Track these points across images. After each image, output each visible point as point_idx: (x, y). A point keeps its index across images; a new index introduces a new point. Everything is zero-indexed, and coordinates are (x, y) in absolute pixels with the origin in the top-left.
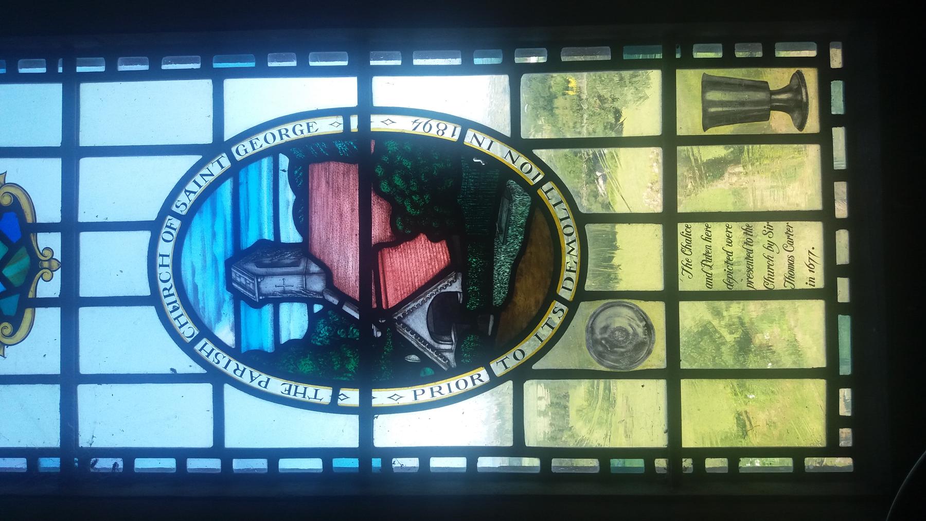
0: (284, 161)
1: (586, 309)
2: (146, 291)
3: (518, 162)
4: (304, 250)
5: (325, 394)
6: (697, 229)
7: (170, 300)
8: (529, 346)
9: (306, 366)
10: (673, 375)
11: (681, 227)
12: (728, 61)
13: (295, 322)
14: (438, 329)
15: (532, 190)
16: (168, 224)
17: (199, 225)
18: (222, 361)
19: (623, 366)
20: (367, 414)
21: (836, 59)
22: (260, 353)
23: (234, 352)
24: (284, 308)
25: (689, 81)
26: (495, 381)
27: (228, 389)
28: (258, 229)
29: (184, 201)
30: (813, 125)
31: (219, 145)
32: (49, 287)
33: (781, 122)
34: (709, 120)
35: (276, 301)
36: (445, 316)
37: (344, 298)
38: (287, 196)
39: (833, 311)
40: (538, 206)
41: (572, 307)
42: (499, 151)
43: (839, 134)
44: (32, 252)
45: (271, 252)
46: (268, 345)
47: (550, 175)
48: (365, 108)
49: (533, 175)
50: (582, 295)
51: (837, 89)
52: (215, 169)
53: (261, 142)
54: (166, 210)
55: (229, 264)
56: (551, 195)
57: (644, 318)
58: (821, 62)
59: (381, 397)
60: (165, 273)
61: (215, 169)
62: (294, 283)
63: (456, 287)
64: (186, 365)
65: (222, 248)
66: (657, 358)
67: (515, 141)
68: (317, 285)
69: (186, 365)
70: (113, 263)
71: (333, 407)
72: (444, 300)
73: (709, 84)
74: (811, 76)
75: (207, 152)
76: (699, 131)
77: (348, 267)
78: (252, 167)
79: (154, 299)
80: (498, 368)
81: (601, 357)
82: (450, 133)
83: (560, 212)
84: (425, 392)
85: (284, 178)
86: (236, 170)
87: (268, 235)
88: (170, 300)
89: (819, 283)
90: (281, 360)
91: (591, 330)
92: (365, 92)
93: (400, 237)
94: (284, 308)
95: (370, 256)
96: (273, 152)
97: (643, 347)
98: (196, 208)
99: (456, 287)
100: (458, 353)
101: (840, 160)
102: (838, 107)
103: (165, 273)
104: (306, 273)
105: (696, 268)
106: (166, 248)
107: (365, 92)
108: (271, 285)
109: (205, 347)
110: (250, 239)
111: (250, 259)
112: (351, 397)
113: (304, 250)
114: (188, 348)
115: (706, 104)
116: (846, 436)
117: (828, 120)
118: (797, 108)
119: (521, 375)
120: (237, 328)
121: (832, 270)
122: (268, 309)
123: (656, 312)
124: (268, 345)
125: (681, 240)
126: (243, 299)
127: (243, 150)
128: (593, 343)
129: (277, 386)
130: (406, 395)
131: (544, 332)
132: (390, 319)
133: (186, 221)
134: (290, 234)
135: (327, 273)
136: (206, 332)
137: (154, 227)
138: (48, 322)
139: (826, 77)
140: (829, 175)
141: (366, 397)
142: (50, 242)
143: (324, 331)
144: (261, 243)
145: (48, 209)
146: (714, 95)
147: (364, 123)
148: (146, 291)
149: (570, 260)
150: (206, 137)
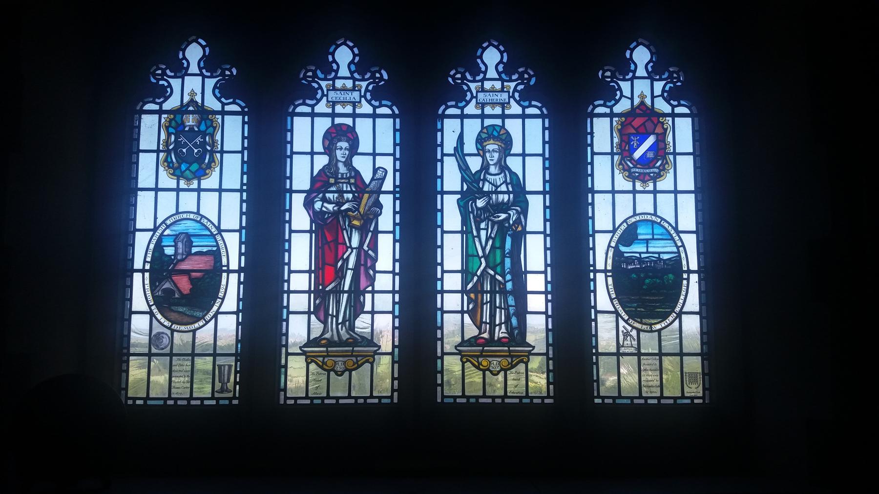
0: (215, 249)
1: (169, 332)
2: (180, 210)
3: (211, 314)
4: (189, 254)
5: (149, 259)
6: (189, 363)
7: (177, 217)
8: (159, 316)
9: (156, 254)
10: (150, 355)
11: (190, 358)
12: (236, 372)
13: (169, 251)
14: (165, 291)
15: (203, 318)
16: (199, 216)
17: (198, 225)
18: (159, 231)
19: (153, 341)
20: (143, 271)
21: (235, 402)
22: (161, 242)
23: (162, 235)
24: (173, 248)
25: (231, 361)
26: (150, 306)
27: (151, 233)
28: (196, 241)
29: (205, 221)
30: (217, 395)
31: (220, 231)
32: (183, 184)
33: (218, 386)
34: (220, 367)
35: (176, 246)
36: (169, 292)
37: (175, 265)
38: (205, 249)
39: (165, 399)
40: (198, 319)
41: (169, 328)
42: (215, 308)
43: (214, 402)
44: (193, 179)
45: (189, 244)
46: (163, 244)
47: (207, 322)
48: (229, 272)
49: (208, 318)
50: (173, 331)
51: (227, 402)
52: (214, 230)
53: (221, 243)
54: (203, 216)
55: (187, 233)
56: (201, 323)
57: (166, 347)
58: (234, 397)
59: (147, 275)
60: (185, 216)
61: (214, 230)
62: (180, 251)
63: (177, 296)
64: (159, 222)
65: (191, 231)
66: (154, 350)
67: (218, 313)
68: (179, 257)
69: (159, 222)
70: (188, 201)
71: (145, 262)
72: (173, 292)
73: (230, 366)
74: (231, 395)
75: (218, 228)
76: (217, 363)
77: (184, 266)
78: (213, 240)
79: (178, 213)
80: (153, 307)
81: (155, 336)
82: (221, 295)
83: (196, 325)
84: (147, 287)
85: (210, 248)
86: (213, 235)
87: (194, 244)
88: (177, 217)
89: (173, 396)
90: (159, 247)
91: (163, 333)
92: (234, 271)
93: (192, 280)
94: (173, 248)
95: (187, 272)
96: (217, 246)
97: (157, 347)
98: (203, 225)
99: (177, 296)
100: (158, 296)
101: (206, 402)
102: (221, 402)
103: (185, 216)
104: (183, 254)
105: (179, 362)
106: (192, 216)
107: (234, 271)
108: (180, 245)
109: (163, 227)
110: (193, 239)
111: (187, 239)
112: (147, 267)
113: (189, 254)
114: (164, 222)
115: (224, 366)
116: (130, 402)
117: (218, 399)
118: (222, 391)
119: (151, 314)
120: (168, 235)
121: (176, 399)
122: (173, 244)
123: (167, 351)
124: (163, 244)
125: (186, 358)
126: (176, 237)
127: (219, 238)
128: (159, 333)
129: (152, 246)
130: (147, 282)
131: (163, 320)
132: (169, 278)
133: (199, 222)
134: (194, 250)
135: (183, 260)
136: (168, 227)
137: (198, 213)
138: (173, 184)
139: (230, 399)
140: (202, 399)
141: (147, 271)
142: (195, 185)
143: (166, 259)
144: (192, 242)
145: (205, 184)
146: (227, 368)
147: (225, 271)
148: (180, 210)
149: (183, 328)
150: (222, 228)
